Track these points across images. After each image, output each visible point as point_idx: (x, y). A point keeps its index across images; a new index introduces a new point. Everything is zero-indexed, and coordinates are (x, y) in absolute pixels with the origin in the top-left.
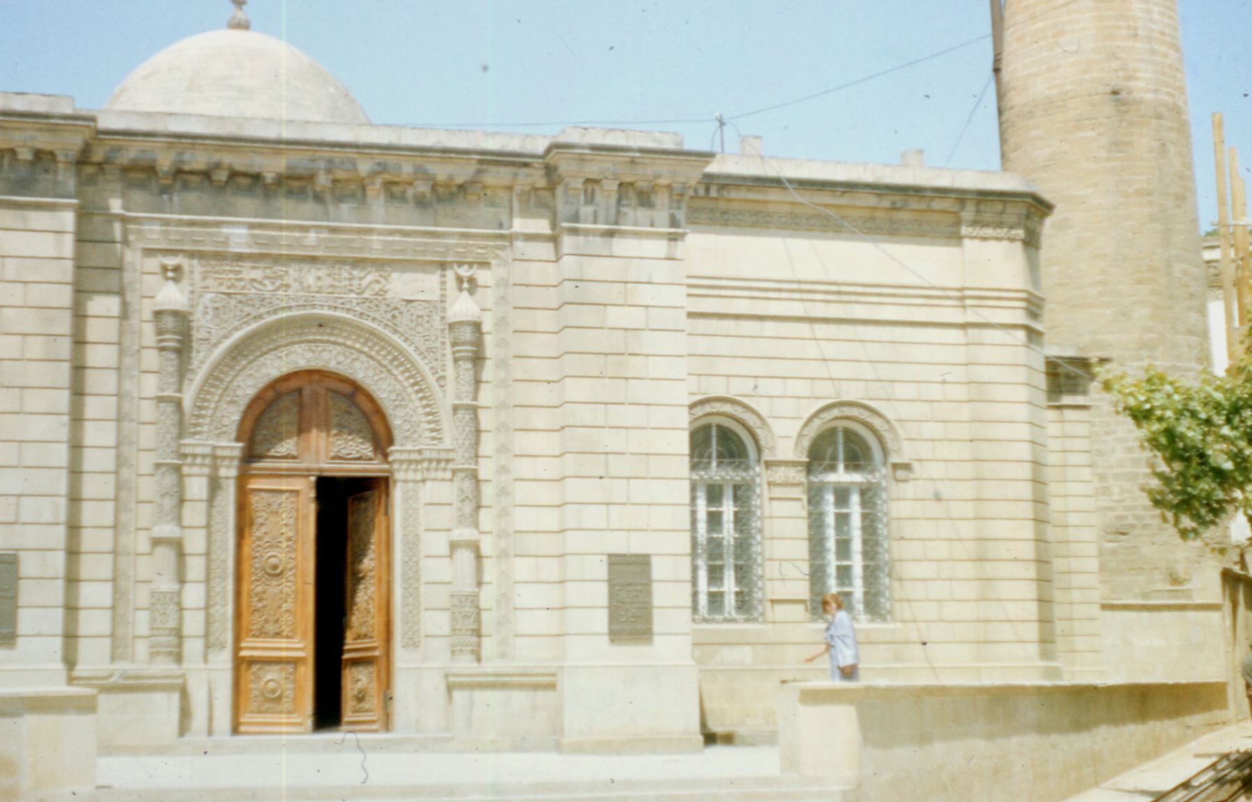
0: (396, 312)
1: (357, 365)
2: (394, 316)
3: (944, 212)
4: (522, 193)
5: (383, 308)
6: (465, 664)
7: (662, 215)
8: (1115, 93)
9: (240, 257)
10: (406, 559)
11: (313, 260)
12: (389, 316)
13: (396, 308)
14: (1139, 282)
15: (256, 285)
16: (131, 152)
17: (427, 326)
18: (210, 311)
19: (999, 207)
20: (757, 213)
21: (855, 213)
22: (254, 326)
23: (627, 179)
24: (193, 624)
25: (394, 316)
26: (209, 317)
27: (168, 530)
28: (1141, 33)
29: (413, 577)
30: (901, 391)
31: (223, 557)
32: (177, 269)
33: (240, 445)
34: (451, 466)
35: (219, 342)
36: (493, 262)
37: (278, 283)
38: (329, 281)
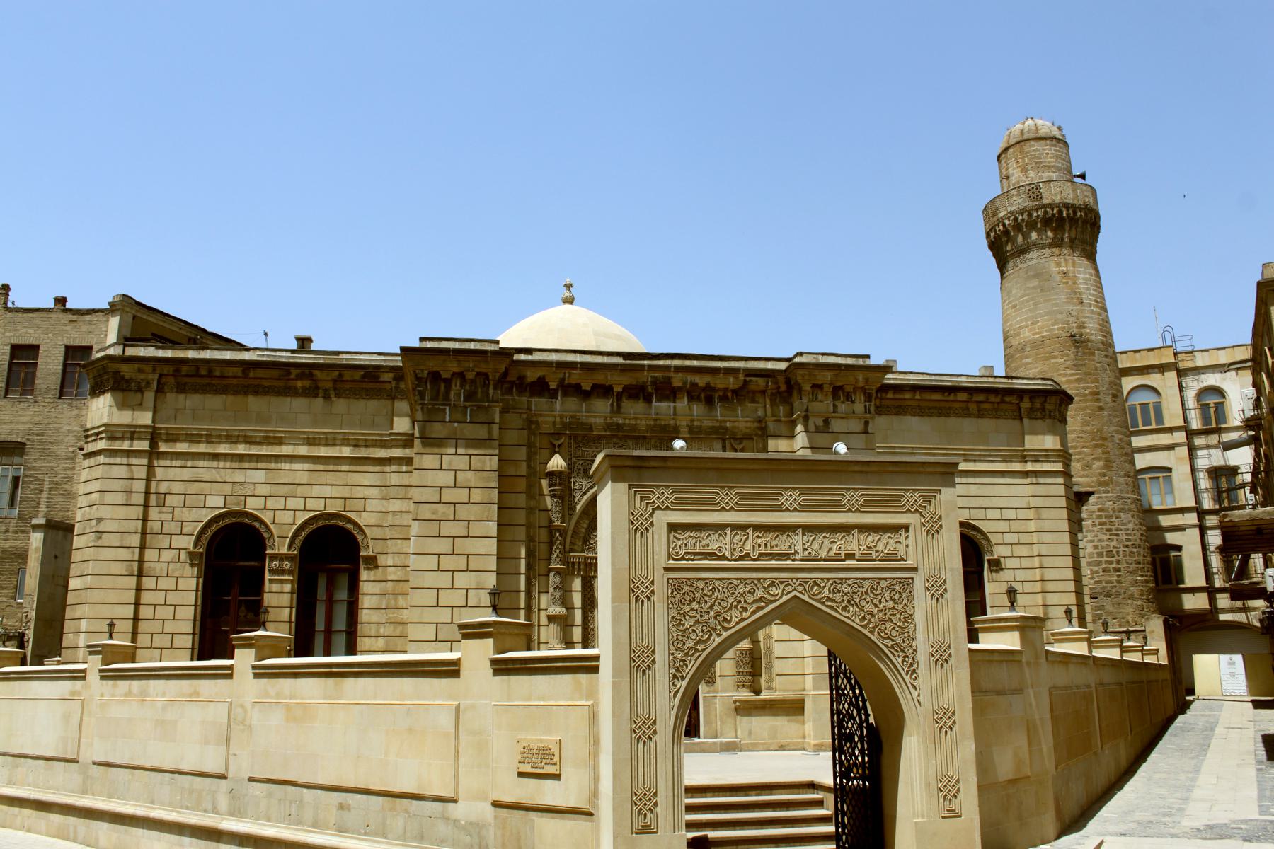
3: (1010, 403)
4: (772, 394)
6: (746, 695)
7: (859, 407)
8: (1072, 336)
9: (599, 438)
11: (644, 437)
14: (1096, 446)
16: (532, 375)
19: (1042, 399)
20: (899, 407)
21: (956, 405)
23: (838, 384)
27: (558, 610)
30: (992, 514)
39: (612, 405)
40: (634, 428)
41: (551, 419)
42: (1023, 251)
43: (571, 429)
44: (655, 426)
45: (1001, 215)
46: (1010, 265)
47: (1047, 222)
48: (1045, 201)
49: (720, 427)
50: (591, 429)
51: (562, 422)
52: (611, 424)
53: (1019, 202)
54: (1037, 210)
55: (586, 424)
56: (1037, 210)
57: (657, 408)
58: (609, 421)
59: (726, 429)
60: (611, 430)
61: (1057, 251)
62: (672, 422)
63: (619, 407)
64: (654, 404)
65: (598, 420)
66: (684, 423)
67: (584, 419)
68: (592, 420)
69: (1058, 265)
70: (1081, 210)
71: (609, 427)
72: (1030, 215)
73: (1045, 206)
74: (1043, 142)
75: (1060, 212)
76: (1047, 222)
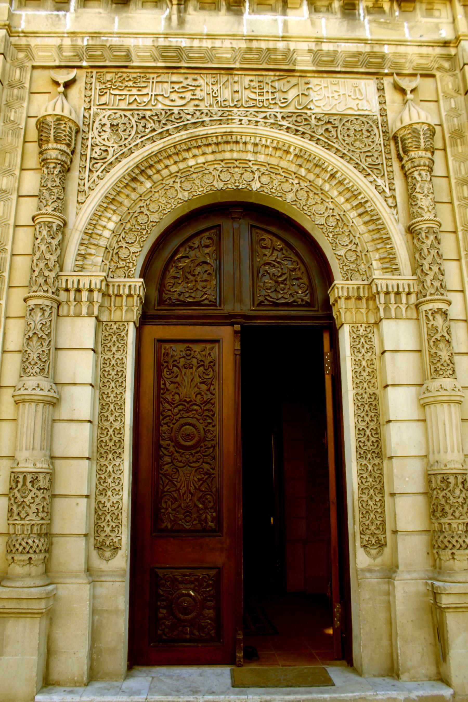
0: (329, 126)
1: (287, 187)
2: (327, 130)
5: (313, 122)
10: (362, 425)
12: (321, 131)
13: (329, 122)
15: (160, 98)
17: (368, 141)
18: (107, 128)
22: (159, 145)
24: (73, 517)
25: (327, 130)
26: (105, 136)
29: (375, 449)
31: (117, 425)
32: (68, 85)
33: (142, 280)
34: (413, 299)
35: (118, 160)
36: (438, 74)
37: (188, 95)
38: (247, 94)
39: (169, 19)
40: (210, 54)
41: (55, 42)
43: (91, 57)
44: (249, 50)
49: (372, 55)
50: (128, 57)
51: (74, 47)
52: (166, 48)
55: (120, 48)
57: (250, 23)
58: (162, 42)
59: (383, 57)
60: (165, 58)
62: (281, 45)
63: (181, 22)
64: (247, 16)
65: (141, 42)
66: (304, 46)
67: (115, 41)
68: (130, 42)
71: (163, 52)
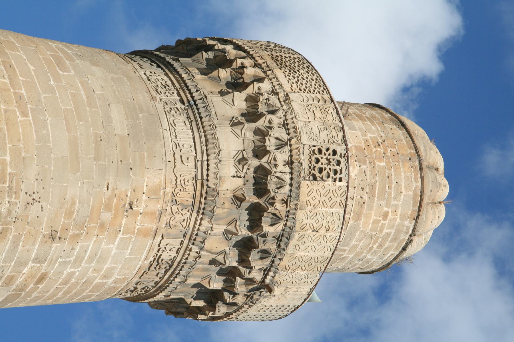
28: (54, 245)
42: (194, 108)
45: (279, 73)
46: (160, 76)
47: (260, 183)
48: (304, 184)
53: (312, 128)
54: (290, 163)
56: (290, 163)
61: (186, 196)
69: (153, 193)
70: (266, 271)
72: (281, 145)
73: (295, 186)
74: (411, 210)
75: (276, 219)
76: (260, 183)
